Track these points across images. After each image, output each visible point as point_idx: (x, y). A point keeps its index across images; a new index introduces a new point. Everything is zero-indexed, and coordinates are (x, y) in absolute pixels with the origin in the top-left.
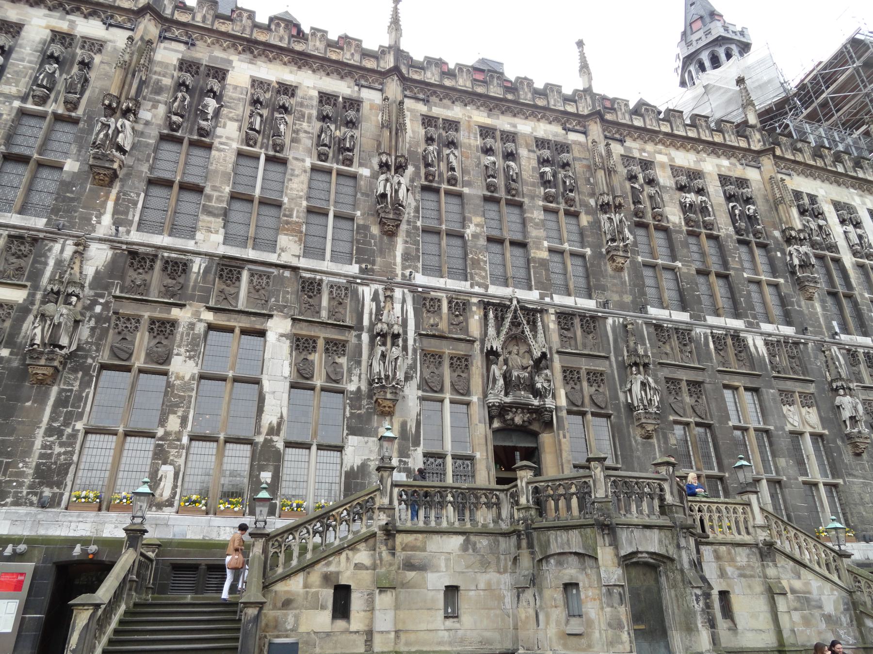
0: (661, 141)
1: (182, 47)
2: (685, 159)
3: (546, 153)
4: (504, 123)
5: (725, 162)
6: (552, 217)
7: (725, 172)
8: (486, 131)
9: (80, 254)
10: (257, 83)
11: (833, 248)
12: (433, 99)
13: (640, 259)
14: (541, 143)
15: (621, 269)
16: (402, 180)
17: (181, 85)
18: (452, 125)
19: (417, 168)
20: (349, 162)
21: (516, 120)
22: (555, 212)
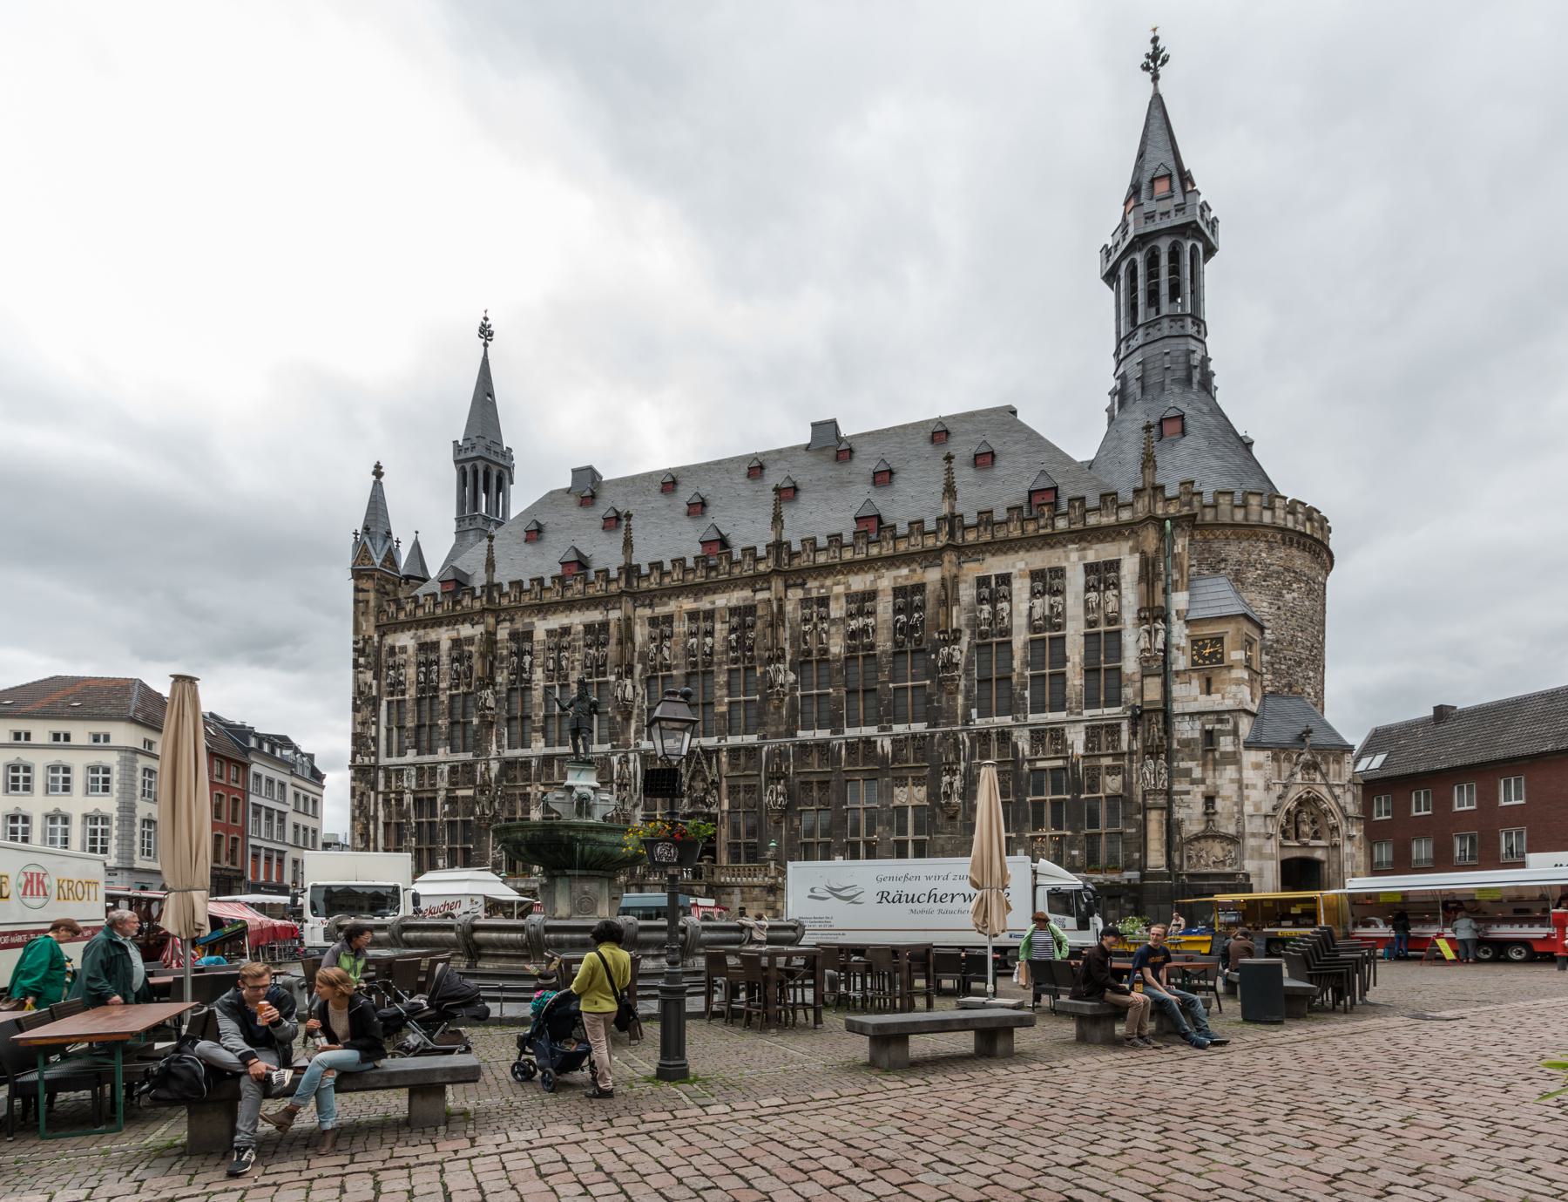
0: (840, 572)
1: (507, 624)
2: (859, 582)
3: (735, 621)
4: (705, 604)
5: (905, 571)
6: (735, 675)
7: (902, 582)
8: (693, 616)
9: (488, 769)
10: (550, 633)
11: (1007, 632)
12: (656, 600)
13: (798, 694)
14: (733, 611)
15: (778, 708)
16: (628, 681)
17: (511, 653)
18: (669, 619)
19: (644, 664)
20: (604, 674)
21: (716, 596)
22: (738, 670)
